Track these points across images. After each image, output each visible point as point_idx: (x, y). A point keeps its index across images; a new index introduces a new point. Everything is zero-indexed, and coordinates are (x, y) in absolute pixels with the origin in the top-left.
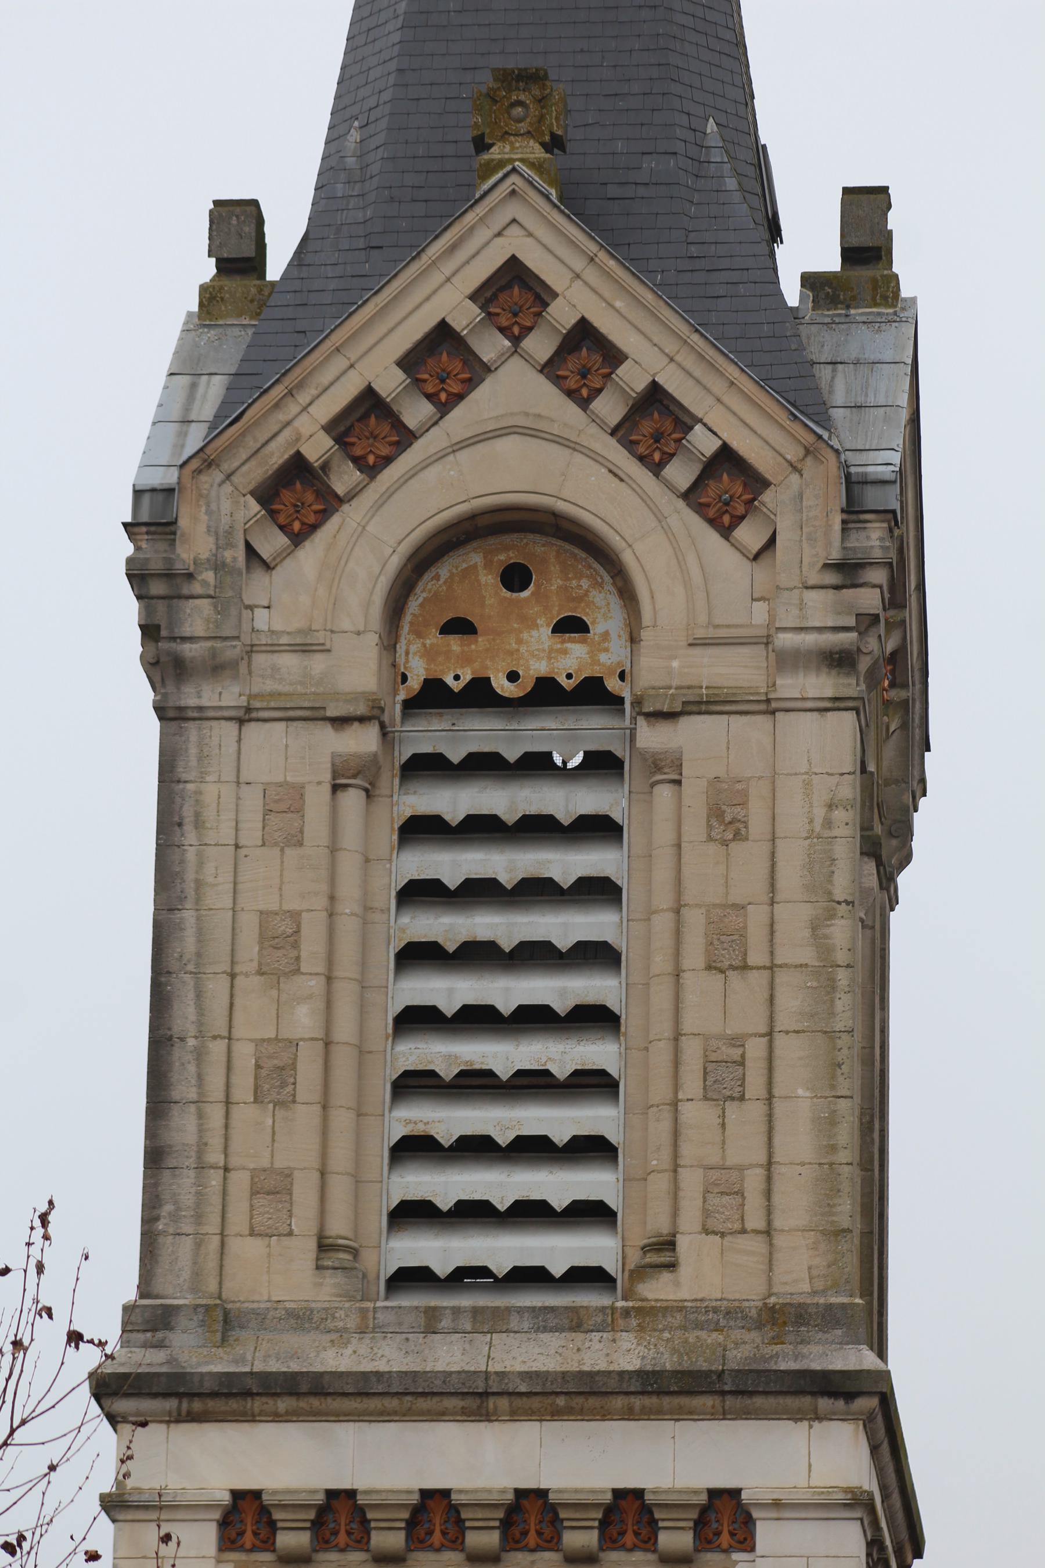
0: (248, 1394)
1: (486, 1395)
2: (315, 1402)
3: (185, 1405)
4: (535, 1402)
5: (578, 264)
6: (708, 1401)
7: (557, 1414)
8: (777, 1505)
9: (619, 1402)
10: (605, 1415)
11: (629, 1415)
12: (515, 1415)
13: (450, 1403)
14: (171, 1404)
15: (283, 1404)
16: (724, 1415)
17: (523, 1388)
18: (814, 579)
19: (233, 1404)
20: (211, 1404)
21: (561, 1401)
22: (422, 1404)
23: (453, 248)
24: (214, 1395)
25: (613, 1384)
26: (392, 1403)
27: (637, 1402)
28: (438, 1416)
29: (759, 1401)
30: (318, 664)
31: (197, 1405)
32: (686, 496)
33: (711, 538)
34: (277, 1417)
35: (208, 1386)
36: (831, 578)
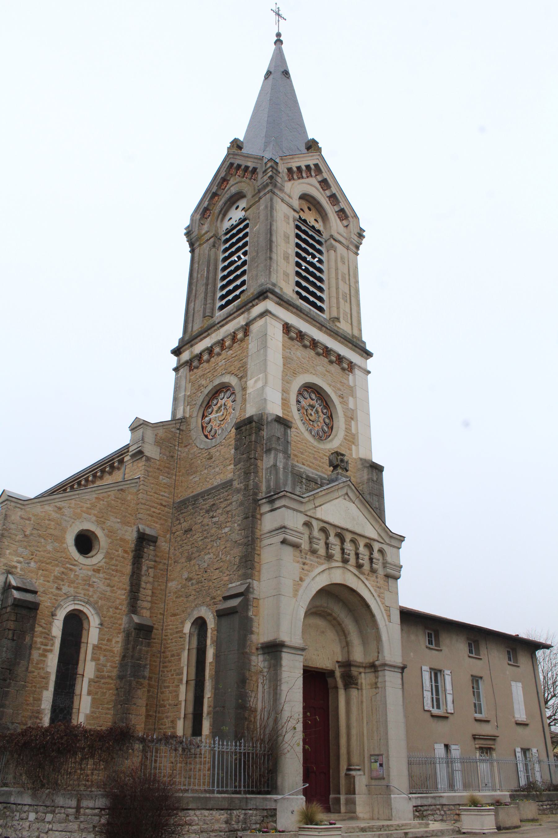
0: (290, 305)
1: (323, 326)
2: (299, 313)
3: (280, 301)
4: (329, 331)
5: (327, 171)
6: (350, 345)
7: (330, 335)
8: (359, 367)
9: (339, 338)
10: (336, 339)
11: (339, 342)
12: (325, 332)
13: (318, 325)
14: (278, 300)
15: (294, 310)
16: (351, 349)
17: (329, 328)
18: (356, 234)
19: (287, 306)
20: (284, 304)
21: (332, 333)
22: (314, 322)
23: (312, 156)
24: (285, 302)
25: (340, 335)
26: (310, 320)
27: (342, 340)
28: (314, 326)
29: (357, 349)
30: (291, 200)
31: (282, 302)
32: (336, 212)
33: (338, 220)
34: (292, 312)
35: (285, 300)
36: (357, 235)
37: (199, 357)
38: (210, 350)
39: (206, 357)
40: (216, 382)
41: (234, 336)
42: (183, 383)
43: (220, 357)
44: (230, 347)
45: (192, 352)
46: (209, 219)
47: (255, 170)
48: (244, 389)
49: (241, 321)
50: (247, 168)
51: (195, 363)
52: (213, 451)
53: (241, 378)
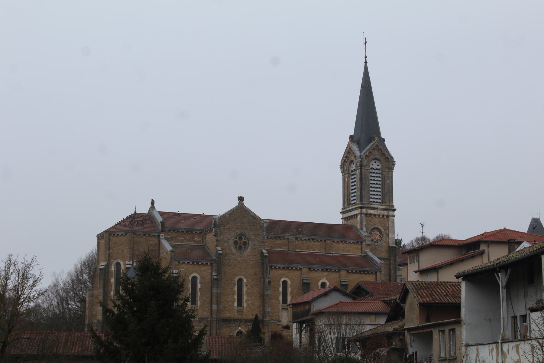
37: (371, 214)
38: (375, 215)
39: (373, 216)
40: (376, 226)
41: (383, 216)
42: (364, 220)
43: (376, 219)
44: (381, 218)
45: (367, 211)
46: (367, 160)
47: (387, 158)
48: (388, 235)
49: (385, 213)
50: (384, 154)
51: (368, 216)
52: (376, 246)
53: (385, 230)
